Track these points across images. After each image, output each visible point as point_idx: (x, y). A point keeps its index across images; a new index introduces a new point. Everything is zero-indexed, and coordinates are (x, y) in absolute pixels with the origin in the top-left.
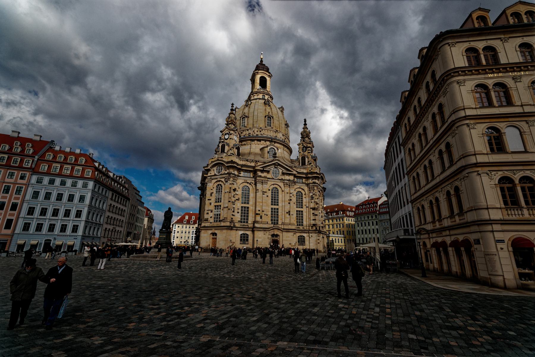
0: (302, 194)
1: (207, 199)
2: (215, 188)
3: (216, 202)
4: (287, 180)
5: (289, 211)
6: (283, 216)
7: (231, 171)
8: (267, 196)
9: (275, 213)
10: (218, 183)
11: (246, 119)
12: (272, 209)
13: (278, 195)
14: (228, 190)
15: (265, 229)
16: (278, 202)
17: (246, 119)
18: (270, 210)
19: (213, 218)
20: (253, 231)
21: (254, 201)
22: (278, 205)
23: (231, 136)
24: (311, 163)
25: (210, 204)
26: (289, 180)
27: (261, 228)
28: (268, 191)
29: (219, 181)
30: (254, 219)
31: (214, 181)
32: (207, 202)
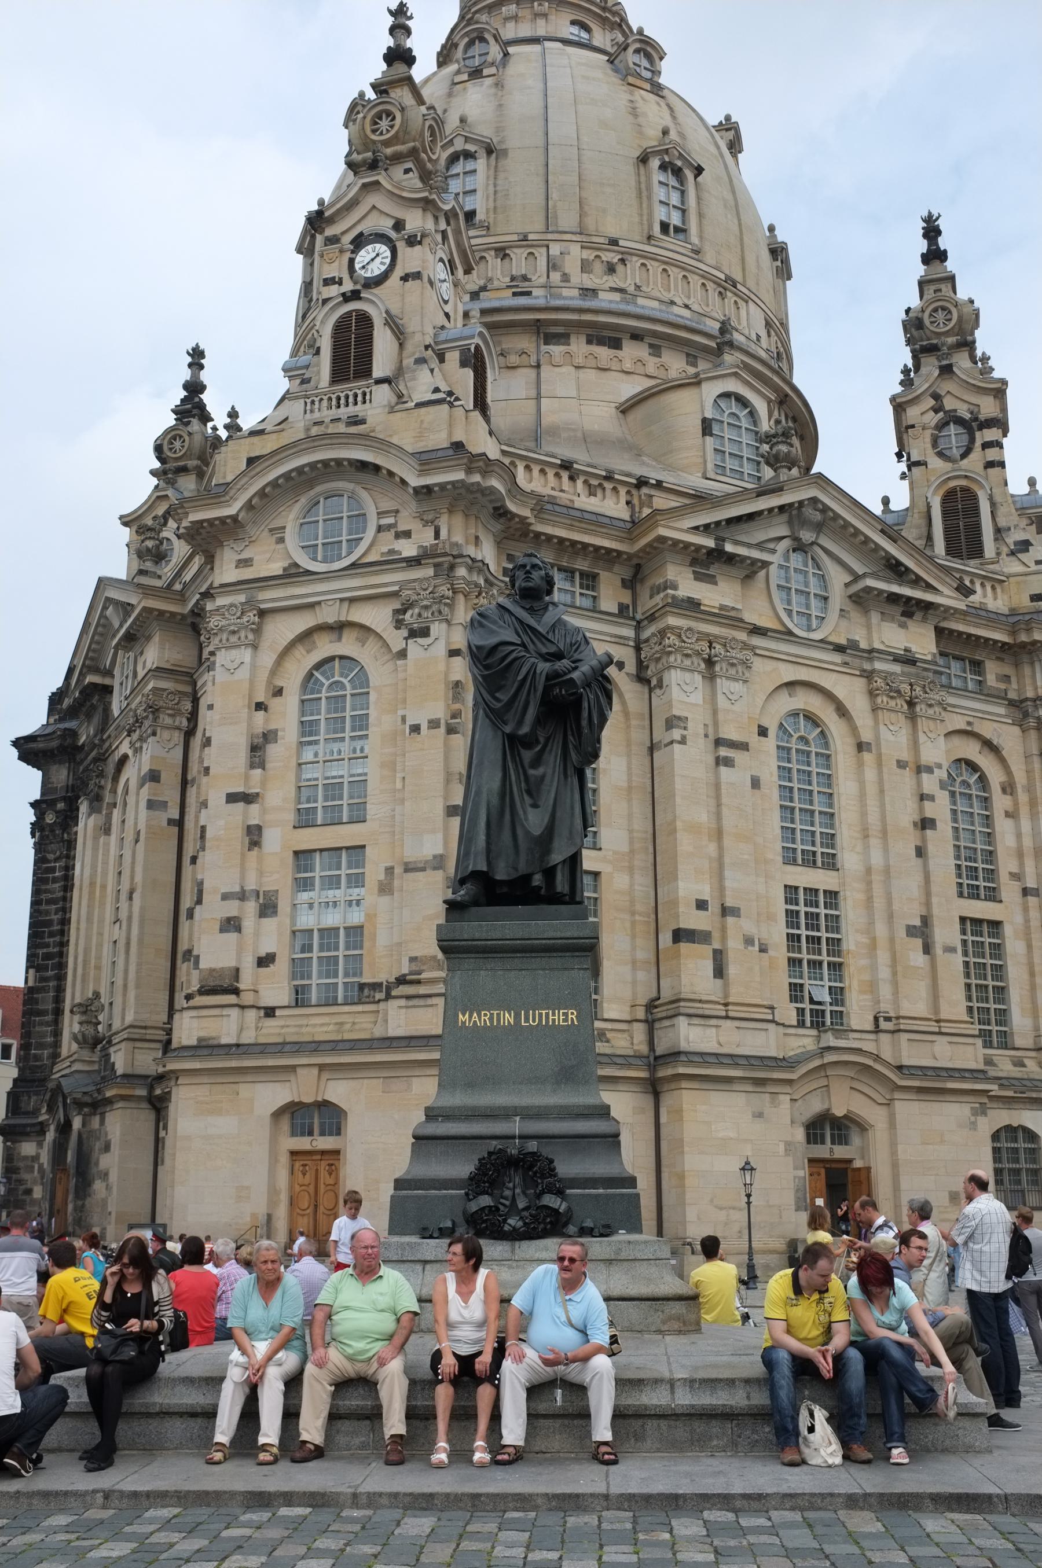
0: (983, 780)
1: (216, 798)
2: (291, 701)
3: (305, 820)
4: (897, 659)
5: (926, 920)
6: (883, 957)
7: (455, 531)
8: (756, 783)
9: (813, 928)
10: (326, 647)
11: (481, 164)
12: (791, 890)
14: (439, 710)
15: (761, 1074)
17: (481, 164)
18: (780, 907)
19: (282, 967)
20: (654, 1088)
21: (641, 824)
22: (831, 863)
23: (411, 258)
24: (1025, 546)
25: (254, 836)
26: (908, 659)
27: (733, 1060)
28: (754, 739)
29: (339, 628)
30: (645, 976)
31: (283, 630)
32: (219, 821)
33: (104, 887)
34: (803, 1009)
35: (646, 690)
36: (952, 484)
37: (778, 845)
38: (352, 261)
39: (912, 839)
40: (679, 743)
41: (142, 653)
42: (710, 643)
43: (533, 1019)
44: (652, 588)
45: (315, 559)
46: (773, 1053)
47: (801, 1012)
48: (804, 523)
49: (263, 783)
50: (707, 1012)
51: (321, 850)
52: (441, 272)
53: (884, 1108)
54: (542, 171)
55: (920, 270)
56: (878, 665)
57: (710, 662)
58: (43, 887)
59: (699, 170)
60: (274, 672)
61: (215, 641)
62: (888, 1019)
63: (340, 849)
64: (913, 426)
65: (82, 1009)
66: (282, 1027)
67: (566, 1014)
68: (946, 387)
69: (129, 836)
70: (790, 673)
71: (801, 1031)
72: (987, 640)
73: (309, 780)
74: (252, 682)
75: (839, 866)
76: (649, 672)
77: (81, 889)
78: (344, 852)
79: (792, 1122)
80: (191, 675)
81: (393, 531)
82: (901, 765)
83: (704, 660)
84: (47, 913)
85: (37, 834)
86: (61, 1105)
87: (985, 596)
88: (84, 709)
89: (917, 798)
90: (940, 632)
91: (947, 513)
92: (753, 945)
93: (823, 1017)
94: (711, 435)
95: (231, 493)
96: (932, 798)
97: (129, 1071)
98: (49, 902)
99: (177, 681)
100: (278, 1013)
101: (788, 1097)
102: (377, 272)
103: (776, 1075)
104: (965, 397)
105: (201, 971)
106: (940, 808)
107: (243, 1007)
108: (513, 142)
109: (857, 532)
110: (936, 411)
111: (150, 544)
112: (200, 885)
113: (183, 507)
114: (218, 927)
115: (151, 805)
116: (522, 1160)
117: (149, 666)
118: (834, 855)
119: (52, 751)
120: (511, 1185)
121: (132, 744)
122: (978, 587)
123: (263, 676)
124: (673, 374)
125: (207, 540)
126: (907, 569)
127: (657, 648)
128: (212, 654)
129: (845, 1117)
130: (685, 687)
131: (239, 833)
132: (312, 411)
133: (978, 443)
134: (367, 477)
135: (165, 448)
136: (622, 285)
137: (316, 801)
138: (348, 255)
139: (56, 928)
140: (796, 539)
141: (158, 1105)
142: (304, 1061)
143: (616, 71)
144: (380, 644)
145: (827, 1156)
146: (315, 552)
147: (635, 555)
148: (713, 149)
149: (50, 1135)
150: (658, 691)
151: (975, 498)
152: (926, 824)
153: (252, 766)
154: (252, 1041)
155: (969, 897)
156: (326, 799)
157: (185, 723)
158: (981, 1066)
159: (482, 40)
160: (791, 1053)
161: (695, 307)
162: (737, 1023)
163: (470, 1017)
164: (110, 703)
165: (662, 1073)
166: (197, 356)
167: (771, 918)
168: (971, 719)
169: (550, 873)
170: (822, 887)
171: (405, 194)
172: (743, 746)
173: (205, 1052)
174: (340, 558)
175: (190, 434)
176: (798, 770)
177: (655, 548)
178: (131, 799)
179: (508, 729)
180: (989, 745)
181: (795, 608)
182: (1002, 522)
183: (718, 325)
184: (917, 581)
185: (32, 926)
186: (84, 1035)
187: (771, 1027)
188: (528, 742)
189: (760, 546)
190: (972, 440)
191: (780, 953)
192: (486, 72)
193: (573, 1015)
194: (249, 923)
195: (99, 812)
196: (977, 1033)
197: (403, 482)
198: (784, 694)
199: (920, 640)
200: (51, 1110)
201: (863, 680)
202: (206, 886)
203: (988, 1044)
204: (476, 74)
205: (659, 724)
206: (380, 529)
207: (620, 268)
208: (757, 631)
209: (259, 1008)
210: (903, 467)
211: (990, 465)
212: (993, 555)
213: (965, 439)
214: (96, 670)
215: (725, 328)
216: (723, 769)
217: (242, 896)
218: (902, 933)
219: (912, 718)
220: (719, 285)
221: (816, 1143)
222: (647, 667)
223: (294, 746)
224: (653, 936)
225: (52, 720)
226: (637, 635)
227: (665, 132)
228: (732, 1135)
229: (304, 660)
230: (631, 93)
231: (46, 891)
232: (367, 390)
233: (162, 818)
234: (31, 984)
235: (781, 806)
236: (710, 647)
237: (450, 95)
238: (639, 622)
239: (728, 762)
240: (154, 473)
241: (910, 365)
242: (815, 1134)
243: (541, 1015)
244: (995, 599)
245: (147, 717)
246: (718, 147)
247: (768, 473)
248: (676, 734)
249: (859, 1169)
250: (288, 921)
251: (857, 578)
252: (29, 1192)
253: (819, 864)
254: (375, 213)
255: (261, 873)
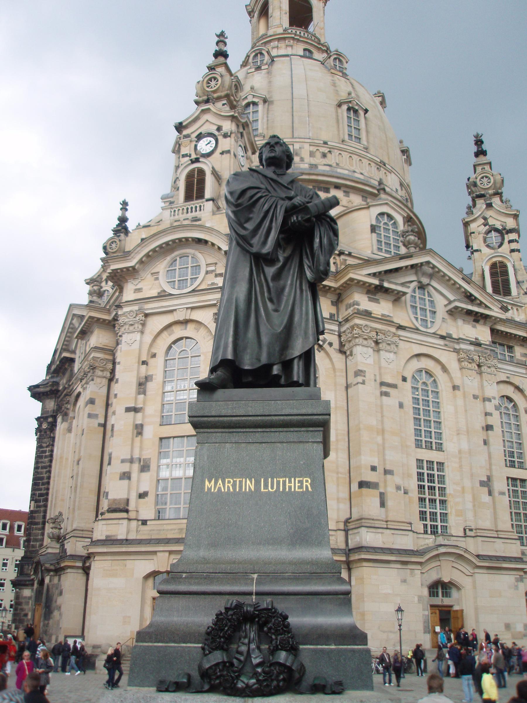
0: (515, 406)
2: (160, 360)
4: (472, 343)
6: (469, 497)
8: (401, 405)
9: (430, 482)
10: (178, 332)
12: (420, 461)
13: (437, 404)
15: (405, 558)
16: (439, 435)
17: (260, 107)
18: (414, 471)
19: (151, 498)
22: (440, 448)
23: (225, 144)
25: (139, 430)
26: (477, 344)
28: (400, 383)
29: (186, 322)
31: (156, 324)
32: (121, 421)
33: (67, 459)
34: (426, 525)
35: (344, 357)
36: (494, 260)
37: (413, 438)
38: (196, 146)
39: (482, 435)
40: (361, 383)
41: (89, 340)
42: (377, 333)
43: (272, 486)
44: (347, 306)
45: (174, 288)
46: (411, 548)
47: (425, 526)
48: (424, 274)
49: (144, 402)
50: (377, 526)
51: (174, 437)
52: (240, 152)
53: (470, 577)
54: (290, 110)
55: (474, 160)
56: (463, 346)
57: (377, 343)
58: (40, 460)
59: (366, 111)
60: (151, 345)
61: (122, 329)
62: (471, 530)
63: (183, 437)
64: (474, 233)
65: (54, 521)
66: (151, 530)
67: (301, 482)
68: (489, 213)
69: (80, 432)
70: (418, 349)
71: (426, 536)
72: (515, 335)
73: (169, 401)
74: (140, 350)
75: (444, 449)
76: (346, 348)
77: (56, 460)
78: (185, 438)
79: (422, 585)
80: (112, 351)
81: (214, 273)
82: (475, 397)
83: (374, 341)
84: (42, 473)
85: (38, 434)
86: (40, 570)
87: (513, 314)
88: (62, 370)
89: (484, 415)
90: (493, 331)
91: (492, 275)
92: (400, 490)
93: (437, 529)
94: (375, 233)
95: (132, 255)
96: (491, 414)
97: (73, 553)
98: (43, 468)
99: (105, 354)
100: (148, 523)
101: (419, 572)
102: (208, 151)
103: (413, 559)
104: (499, 219)
105: (109, 500)
106: (495, 420)
107: (129, 520)
108: (276, 97)
109: (450, 279)
110: (485, 225)
111: (96, 288)
112: (110, 455)
113: (108, 262)
114: (118, 477)
115: (90, 416)
116: (258, 616)
117: (92, 346)
118: (441, 444)
119: (47, 392)
120: (246, 641)
121: (82, 386)
122: (510, 308)
123: (146, 347)
124: (355, 204)
125: (119, 278)
126: (476, 298)
127: (350, 335)
128: (121, 336)
129: (450, 582)
130: (365, 355)
131: (131, 428)
132: (174, 215)
133: (506, 240)
134: (201, 247)
135: (108, 247)
136: (330, 163)
137: (171, 412)
138: (194, 143)
139: (45, 481)
140: (420, 282)
141: (87, 571)
142: (161, 549)
143: (326, 67)
144: (206, 331)
145: (440, 603)
146: (174, 285)
147: (338, 288)
148: (372, 103)
149: (36, 585)
150: (350, 358)
151: (505, 266)
152: (489, 428)
153: (139, 393)
154: (134, 538)
155: (510, 467)
156: (177, 410)
157: (108, 375)
158: (520, 555)
159: (261, 54)
160: (421, 548)
161: (366, 174)
162: (393, 531)
163: (216, 483)
164: (74, 367)
165: (352, 558)
166: (125, 205)
167: (409, 476)
168: (509, 375)
169: (287, 365)
170: (435, 461)
171: (222, 114)
172: (395, 386)
173: (110, 543)
174: (186, 287)
175: (120, 241)
176: (423, 400)
177: (348, 284)
178: (81, 414)
179: (254, 250)
180: (517, 388)
181: (419, 317)
182: (520, 279)
183: (377, 183)
184: (481, 304)
185: (34, 479)
186: (53, 534)
187: (411, 533)
188: (270, 259)
189: (403, 284)
190: (503, 239)
191: (415, 494)
192: (263, 68)
193: (307, 482)
194: (134, 476)
195: (67, 421)
196: (517, 537)
197: (219, 248)
198: (415, 361)
199: (483, 333)
200: (36, 572)
201: (455, 354)
202: (113, 455)
203: (522, 544)
204: (258, 68)
205: (351, 374)
206: (207, 272)
207: (329, 155)
208: (400, 327)
209: (138, 520)
210: (469, 253)
211: (512, 251)
212: (516, 294)
213: (499, 240)
214: (67, 350)
215: (380, 183)
216: (384, 398)
217: (131, 461)
218: (478, 484)
219: (480, 373)
220: (377, 164)
221: (434, 596)
222: (344, 345)
223: (161, 383)
224: (348, 485)
225: (48, 378)
226: (339, 329)
227: (349, 94)
228: (390, 591)
229: (167, 339)
230: (333, 77)
231: (42, 462)
232: (201, 204)
233: (95, 422)
234: (32, 509)
235: (414, 418)
236: (377, 335)
237: (246, 78)
238: (340, 323)
239: (386, 394)
240: (103, 260)
241: (471, 204)
242: (433, 592)
243: (278, 483)
244: (519, 315)
245: (89, 372)
246: (375, 102)
247: (403, 250)
248: (360, 379)
249: (457, 611)
250: (155, 475)
251: (450, 302)
252: (26, 615)
253: (434, 448)
254: (207, 123)
255: (141, 448)
